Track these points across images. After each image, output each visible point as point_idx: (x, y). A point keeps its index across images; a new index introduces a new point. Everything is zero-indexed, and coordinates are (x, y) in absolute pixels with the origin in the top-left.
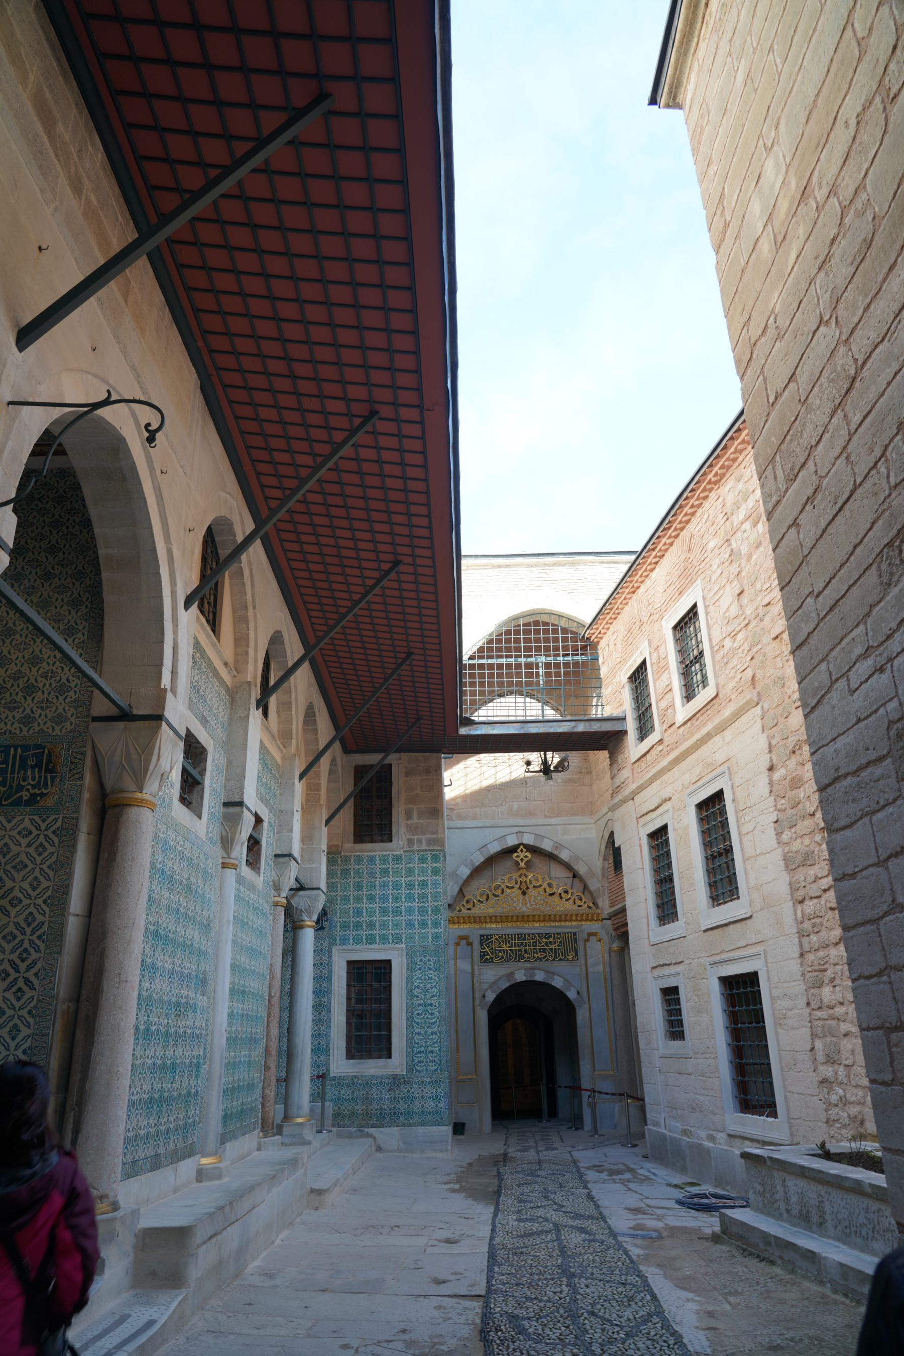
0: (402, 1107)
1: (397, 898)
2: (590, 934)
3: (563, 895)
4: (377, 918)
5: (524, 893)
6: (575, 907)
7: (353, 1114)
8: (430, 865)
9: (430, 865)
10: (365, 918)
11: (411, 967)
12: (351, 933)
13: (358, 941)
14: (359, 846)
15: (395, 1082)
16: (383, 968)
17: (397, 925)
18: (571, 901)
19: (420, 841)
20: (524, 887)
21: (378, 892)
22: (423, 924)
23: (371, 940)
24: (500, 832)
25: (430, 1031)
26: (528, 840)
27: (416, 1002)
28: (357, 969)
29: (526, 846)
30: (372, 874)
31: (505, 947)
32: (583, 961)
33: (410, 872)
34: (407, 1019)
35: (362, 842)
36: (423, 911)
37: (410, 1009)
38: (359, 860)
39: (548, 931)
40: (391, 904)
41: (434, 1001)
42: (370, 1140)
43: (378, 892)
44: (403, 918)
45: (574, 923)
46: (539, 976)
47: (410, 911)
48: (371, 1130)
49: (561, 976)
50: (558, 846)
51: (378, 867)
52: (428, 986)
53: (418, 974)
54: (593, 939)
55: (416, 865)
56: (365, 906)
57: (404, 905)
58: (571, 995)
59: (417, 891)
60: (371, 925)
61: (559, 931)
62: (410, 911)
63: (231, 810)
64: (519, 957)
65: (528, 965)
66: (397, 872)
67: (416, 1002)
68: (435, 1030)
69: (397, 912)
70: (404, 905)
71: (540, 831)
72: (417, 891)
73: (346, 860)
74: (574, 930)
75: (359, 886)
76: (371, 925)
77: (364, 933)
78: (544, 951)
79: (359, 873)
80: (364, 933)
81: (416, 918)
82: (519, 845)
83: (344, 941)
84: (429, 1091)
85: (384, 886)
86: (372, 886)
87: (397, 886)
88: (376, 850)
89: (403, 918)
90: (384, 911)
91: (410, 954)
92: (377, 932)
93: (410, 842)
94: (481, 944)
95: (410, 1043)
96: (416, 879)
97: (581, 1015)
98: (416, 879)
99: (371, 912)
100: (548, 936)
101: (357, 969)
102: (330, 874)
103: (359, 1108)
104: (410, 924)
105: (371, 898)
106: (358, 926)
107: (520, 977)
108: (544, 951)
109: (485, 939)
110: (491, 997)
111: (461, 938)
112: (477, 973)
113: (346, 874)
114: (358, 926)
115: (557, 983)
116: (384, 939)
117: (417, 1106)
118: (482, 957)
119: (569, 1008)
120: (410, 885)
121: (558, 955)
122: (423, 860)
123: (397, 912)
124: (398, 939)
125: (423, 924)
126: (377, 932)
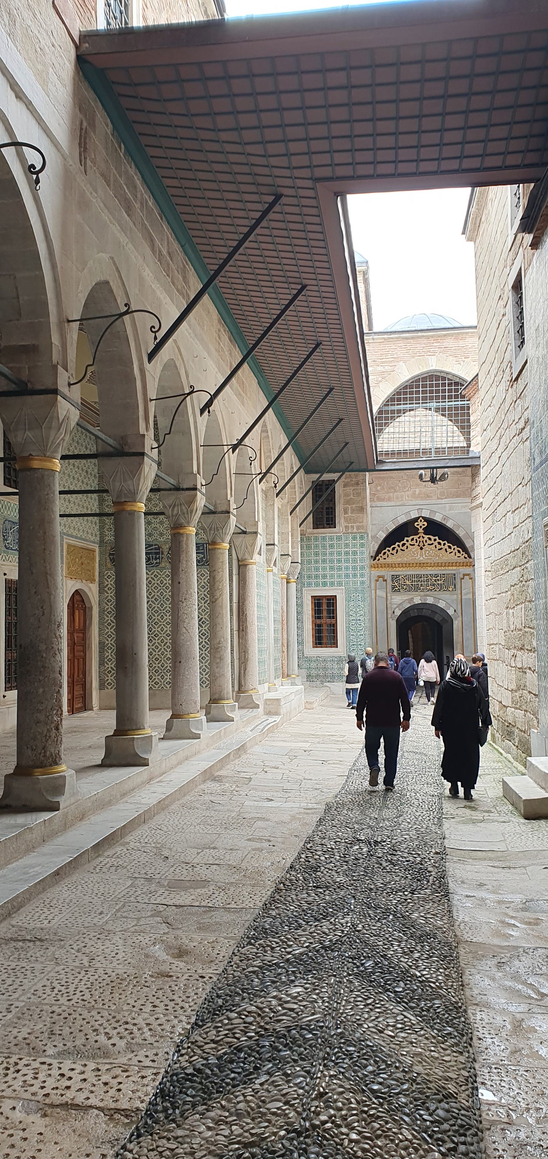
2: (464, 575)
3: (448, 550)
4: (328, 572)
5: (421, 549)
6: (456, 557)
8: (358, 541)
9: (358, 541)
11: (348, 600)
12: (313, 581)
13: (317, 585)
16: (332, 601)
17: (339, 576)
18: (453, 554)
19: (352, 527)
20: (421, 544)
22: (355, 576)
23: (325, 584)
24: (406, 509)
26: (426, 514)
27: (351, 618)
28: (317, 601)
29: (423, 517)
30: (324, 547)
31: (408, 583)
32: (459, 592)
33: (347, 545)
37: (348, 622)
39: (436, 572)
40: (336, 564)
41: (362, 618)
43: (328, 557)
44: (343, 572)
45: (454, 568)
46: (430, 600)
47: (347, 568)
49: (444, 601)
50: (446, 518)
51: (328, 543)
54: (467, 577)
55: (350, 541)
57: (343, 565)
58: (451, 612)
60: (324, 576)
61: (444, 572)
62: (347, 568)
63: (270, 547)
64: (417, 589)
65: (422, 593)
66: (339, 546)
67: (351, 618)
69: (340, 569)
70: (343, 565)
71: (434, 508)
72: (351, 557)
73: (309, 539)
74: (454, 572)
75: (317, 554)
76: (324, 576)
77: (321, 580)
78: (434, 585)
80: (321, 580)
81: (350, 572)
82: (419, 518)
83: (309, 585)
88: (327, 532)
89: (343, 572)
91: (348, 592)
92: (328, 580)
93: (346, 527)
94: (393, 581)
95: (348, 640)
96: (351, 550)
97: (456, 624)
99: (324, 569)
100: (436, 576)
101: (317, 601)
102: (302, 554)
103: (321, 673)
104: (347, 576)
105: (324, 561)
106: (317, 577)
107: (417, 601)
108: (434, 585)
109: (394, 578)
110: (398, 612)
111: (379, 577)
112: (389, 598)
113: (309, 547)
114: (317, 577)
115: (442, 604)
116: (332, 584)
118: (393, 588)
119: (449, 620)
121: (443, 588)
122: (354, 538)
123: (340, 569)
124: (340, 584)
126: (328, 580)
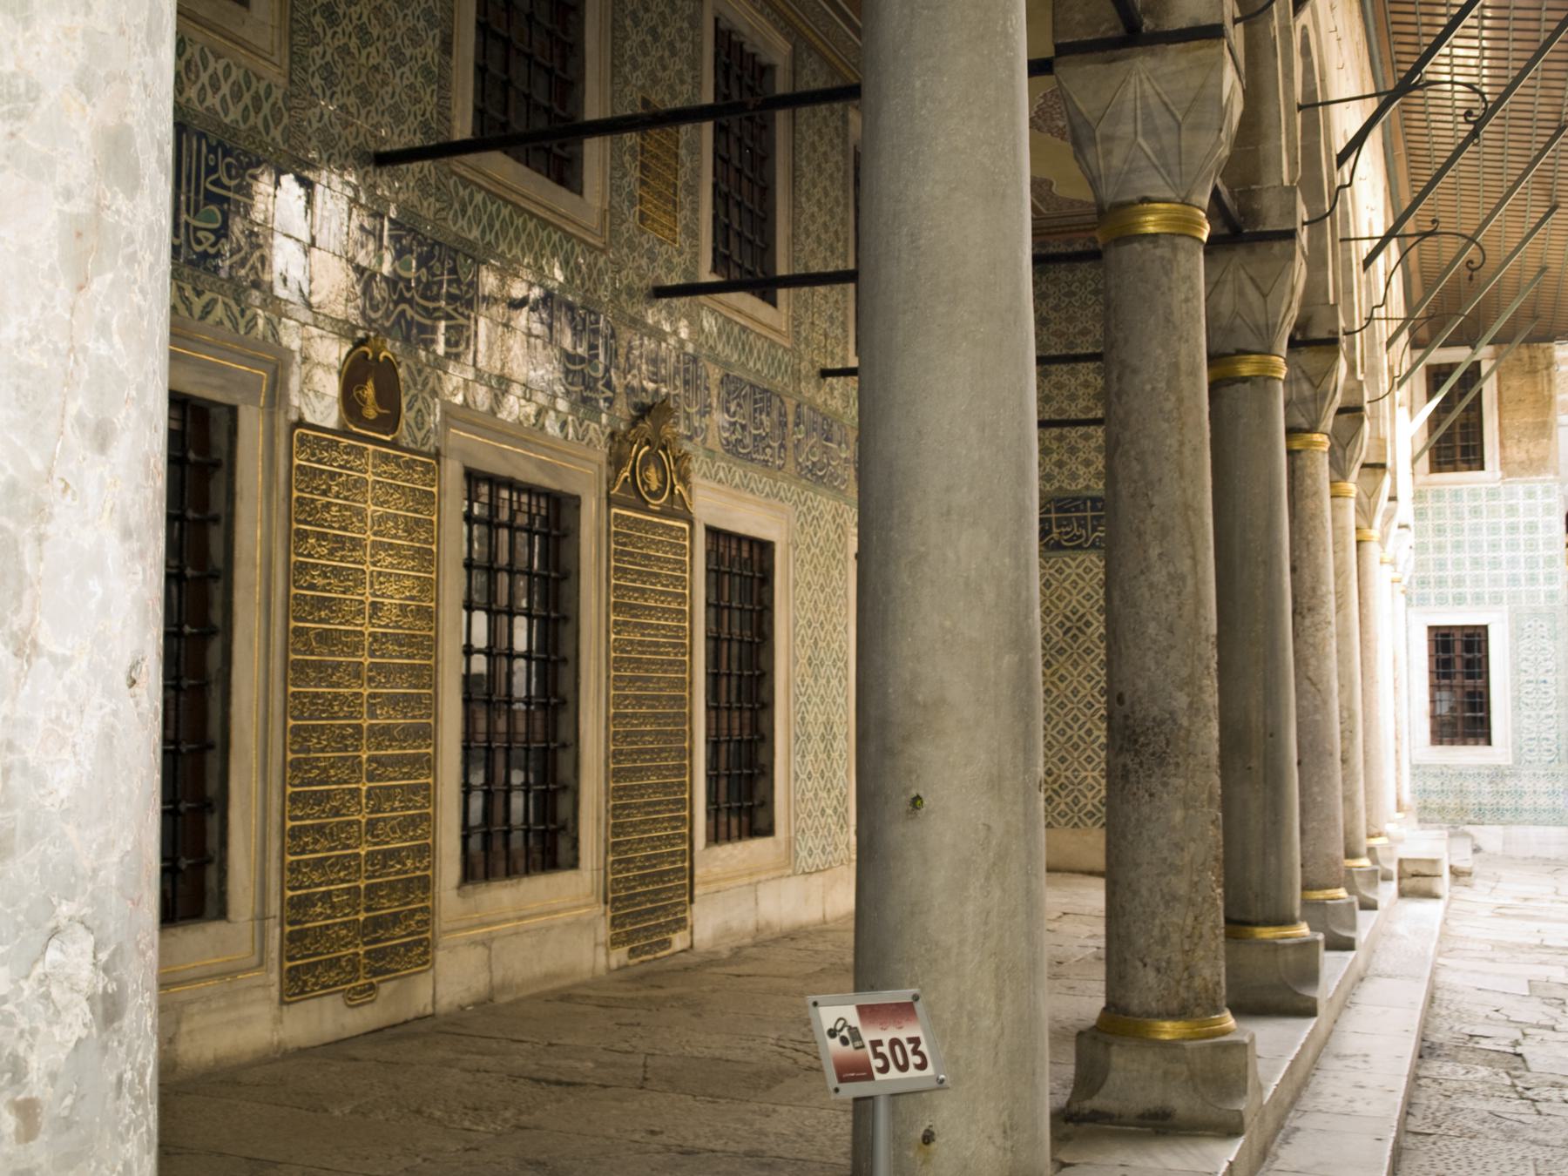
0: (1507, 802)
1: (1494, 546)
7: (1442, 810)
10: (1450, 573)
11: (1517, 634)
13: (1441, 600)
14: (1438, 477)
15: (1497, 774)
17: (1495, 581)
21: (1467, 537)
22: (1532, 579)
23: (1459, 599)
25: (1543, 713)
27: (1524, 677)
30: (1458, 515)
33: (1512, 510)
34: (1513, 698)
35: (1440, 471)
36: (1532, 563)
38: (1438, 496)
40: (1486, 554)
41: (1550, 678)
42: (1468, 842)
48: (1468, 828)
52: (1541, 658)
53: (1525, 643)
56: (1449, 555)
59: (1522, 537)
60: (1459, 581)
68: (1551, 712)
69: (1495, 564)
70: (1504, 554)
72: (1522, 537)
77: (1450, 591)
79: (1439, 513)
80: (1450, 591)
81: (1522, 571)
84: (1543, 785)
85: (1476, 529)
86: (1459, 530)
87: (1494, 529)
90: (1476, 563)
95: (1517, 731)
96: (1522, 520)
98: (1522, 520)
99: (1458, 564)
103: (1451, 802)
104: (1514, 580)
106: (1440, 582)
116: (1478, 598)
117: (1527, 802)
120: (1513, 528)
123: (1495, 564)
124: (1496, 599)
125: (1532, 579)
